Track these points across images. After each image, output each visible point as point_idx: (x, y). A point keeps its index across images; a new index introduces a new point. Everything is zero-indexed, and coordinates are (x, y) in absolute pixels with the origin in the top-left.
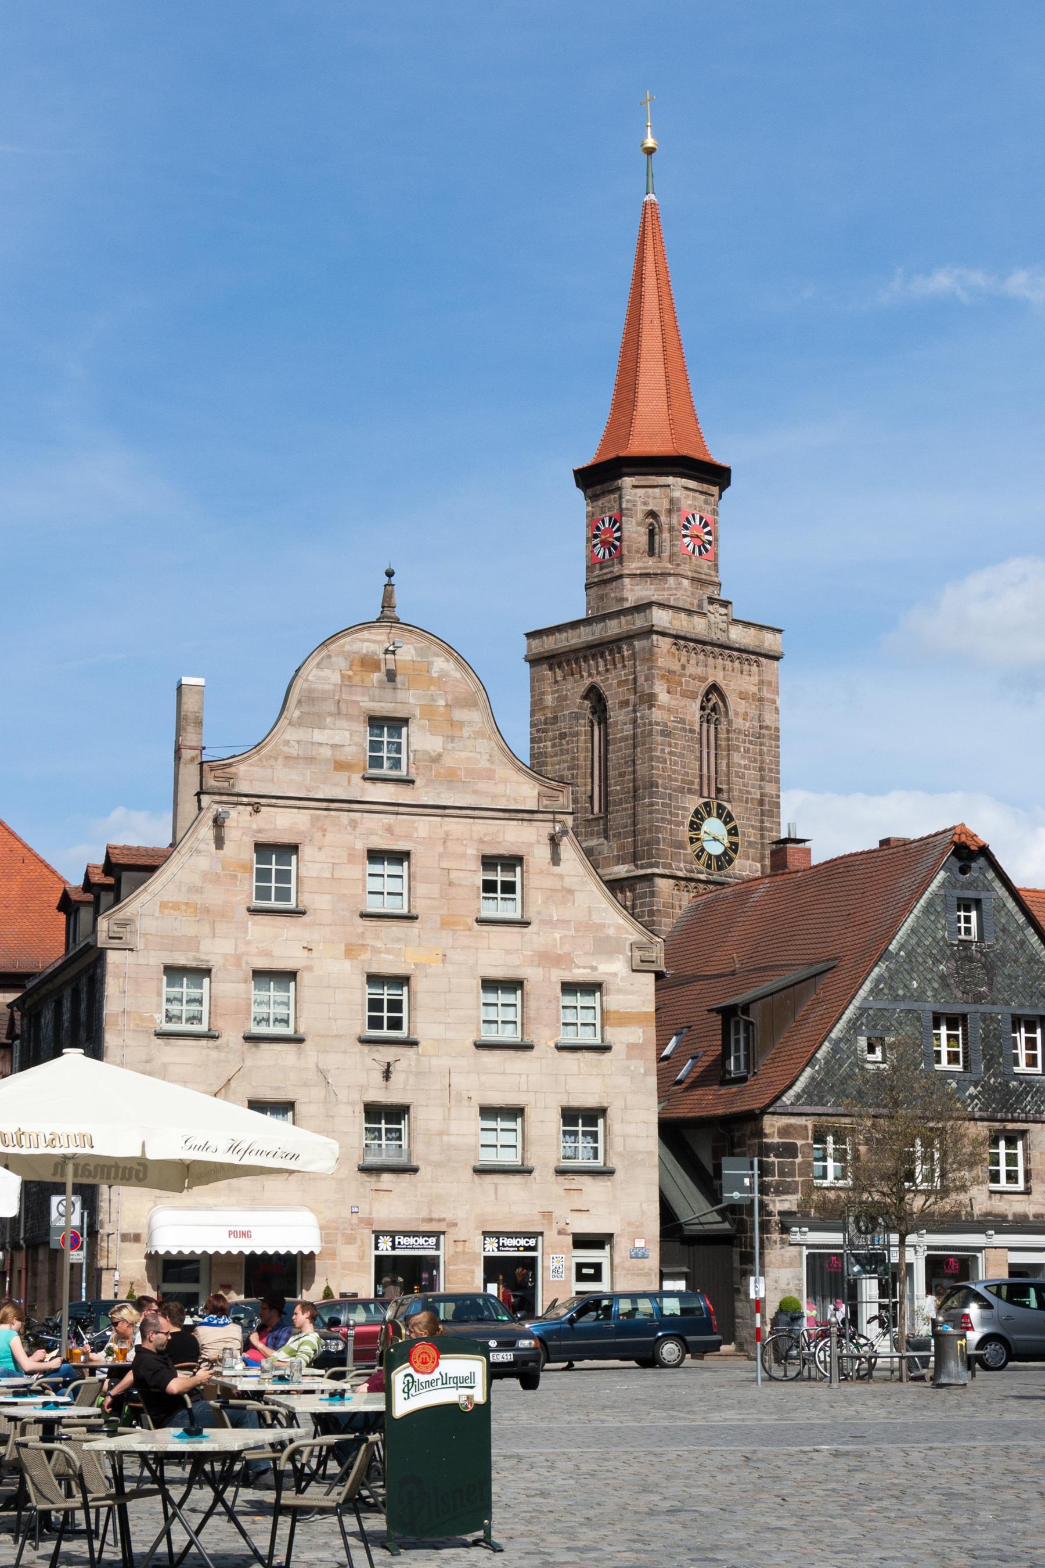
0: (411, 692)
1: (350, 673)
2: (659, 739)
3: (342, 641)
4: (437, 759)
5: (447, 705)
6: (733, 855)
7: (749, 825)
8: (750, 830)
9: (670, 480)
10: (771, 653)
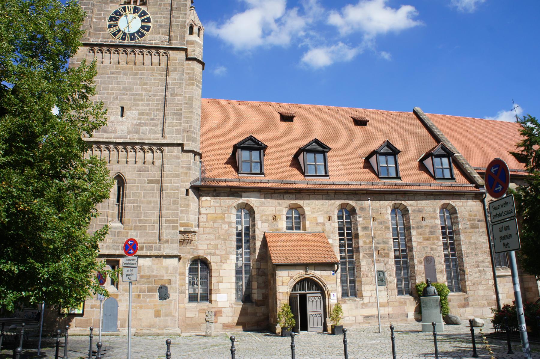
6: (146, 32)
8: (162, 19)
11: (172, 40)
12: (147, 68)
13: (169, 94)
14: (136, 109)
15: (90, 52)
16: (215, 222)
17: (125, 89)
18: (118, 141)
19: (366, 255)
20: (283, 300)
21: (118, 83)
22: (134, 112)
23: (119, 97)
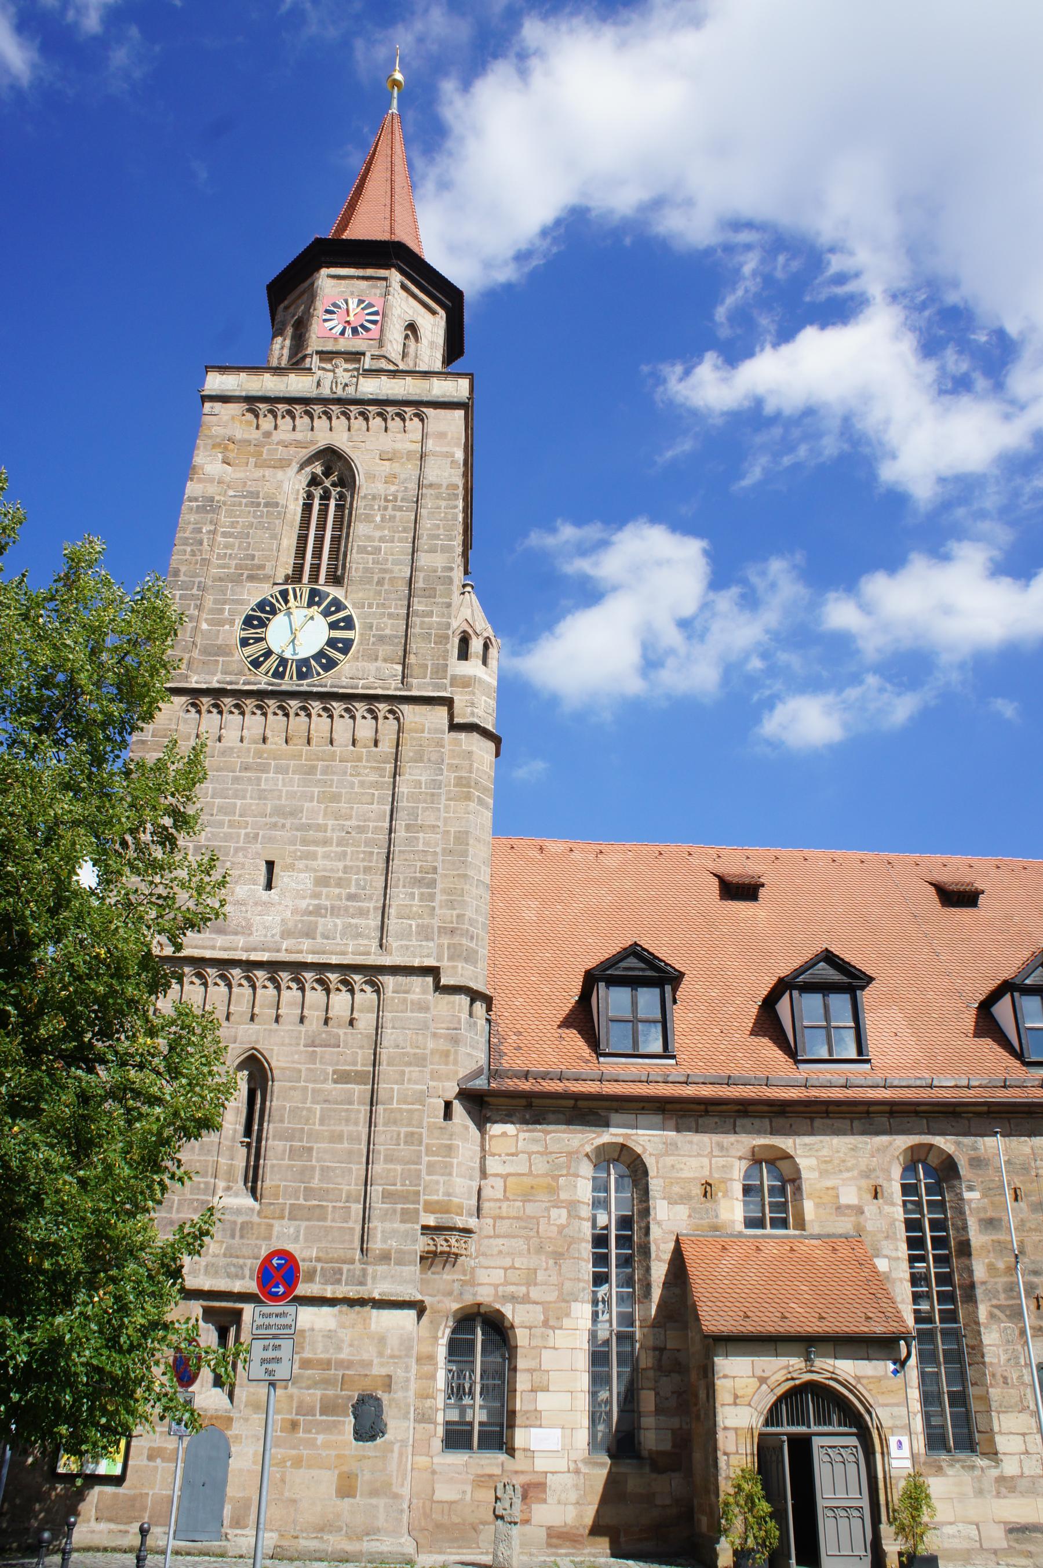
2: (192, 518)
6: (341, 656)
7: (383, 614)
8: (385, 620)
10: (441, 399)
11: (411, 677)
12: (341, 752)
13: (400, 825)
14: (307, 869)
15: (188, 711)
16: (529, 1201)
17: (278, 811)
18: (254, 957)
19: (996, 1312)
20: (737, 1453)
21: (262, 795)
22: (302, 875)
23: (261, 833)
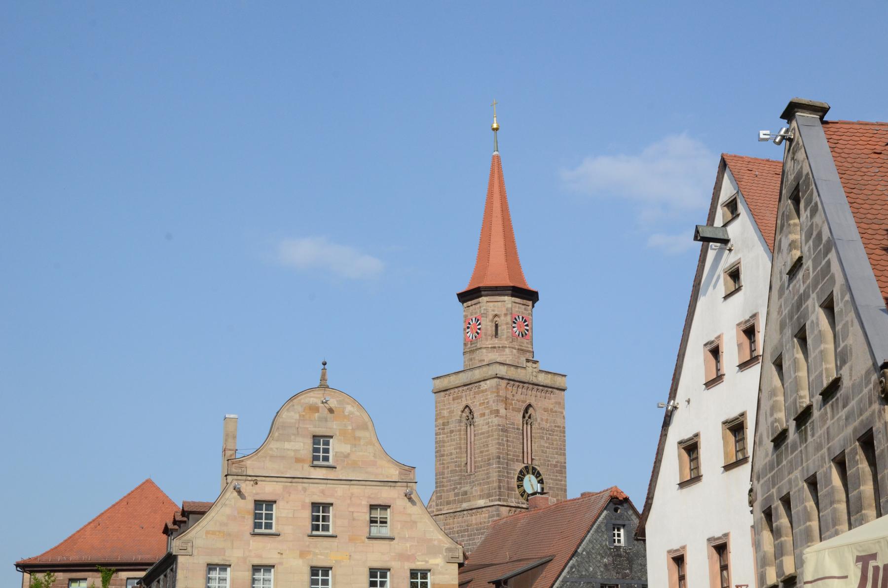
0: (335, 422)
1: (304, 413)
3: (300, 398)
4: (347, 456)
5: (352, 429)
8: (550, 481)
9: (506, 298)
